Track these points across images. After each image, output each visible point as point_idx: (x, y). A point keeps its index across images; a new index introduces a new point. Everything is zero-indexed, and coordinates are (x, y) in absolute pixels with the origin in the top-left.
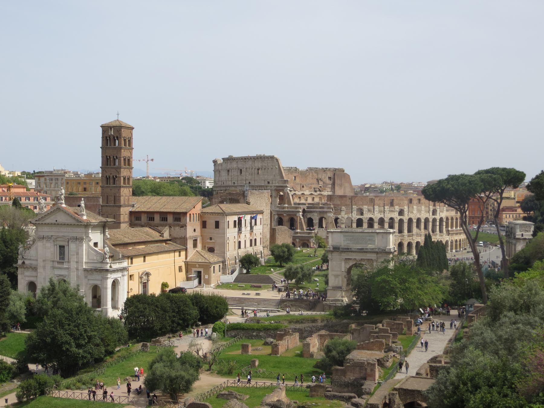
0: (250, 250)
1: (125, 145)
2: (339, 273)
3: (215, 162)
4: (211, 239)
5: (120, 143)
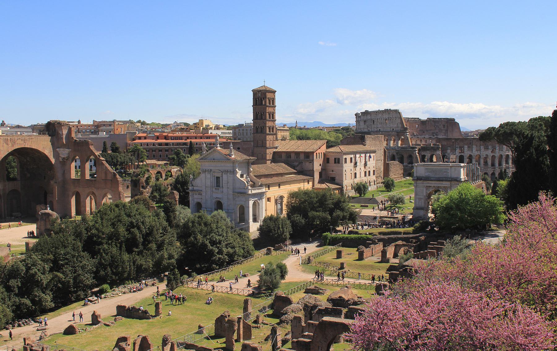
0: (364, 179)
2: (422, 197)
3: (356, 115)
5: (265, 102)
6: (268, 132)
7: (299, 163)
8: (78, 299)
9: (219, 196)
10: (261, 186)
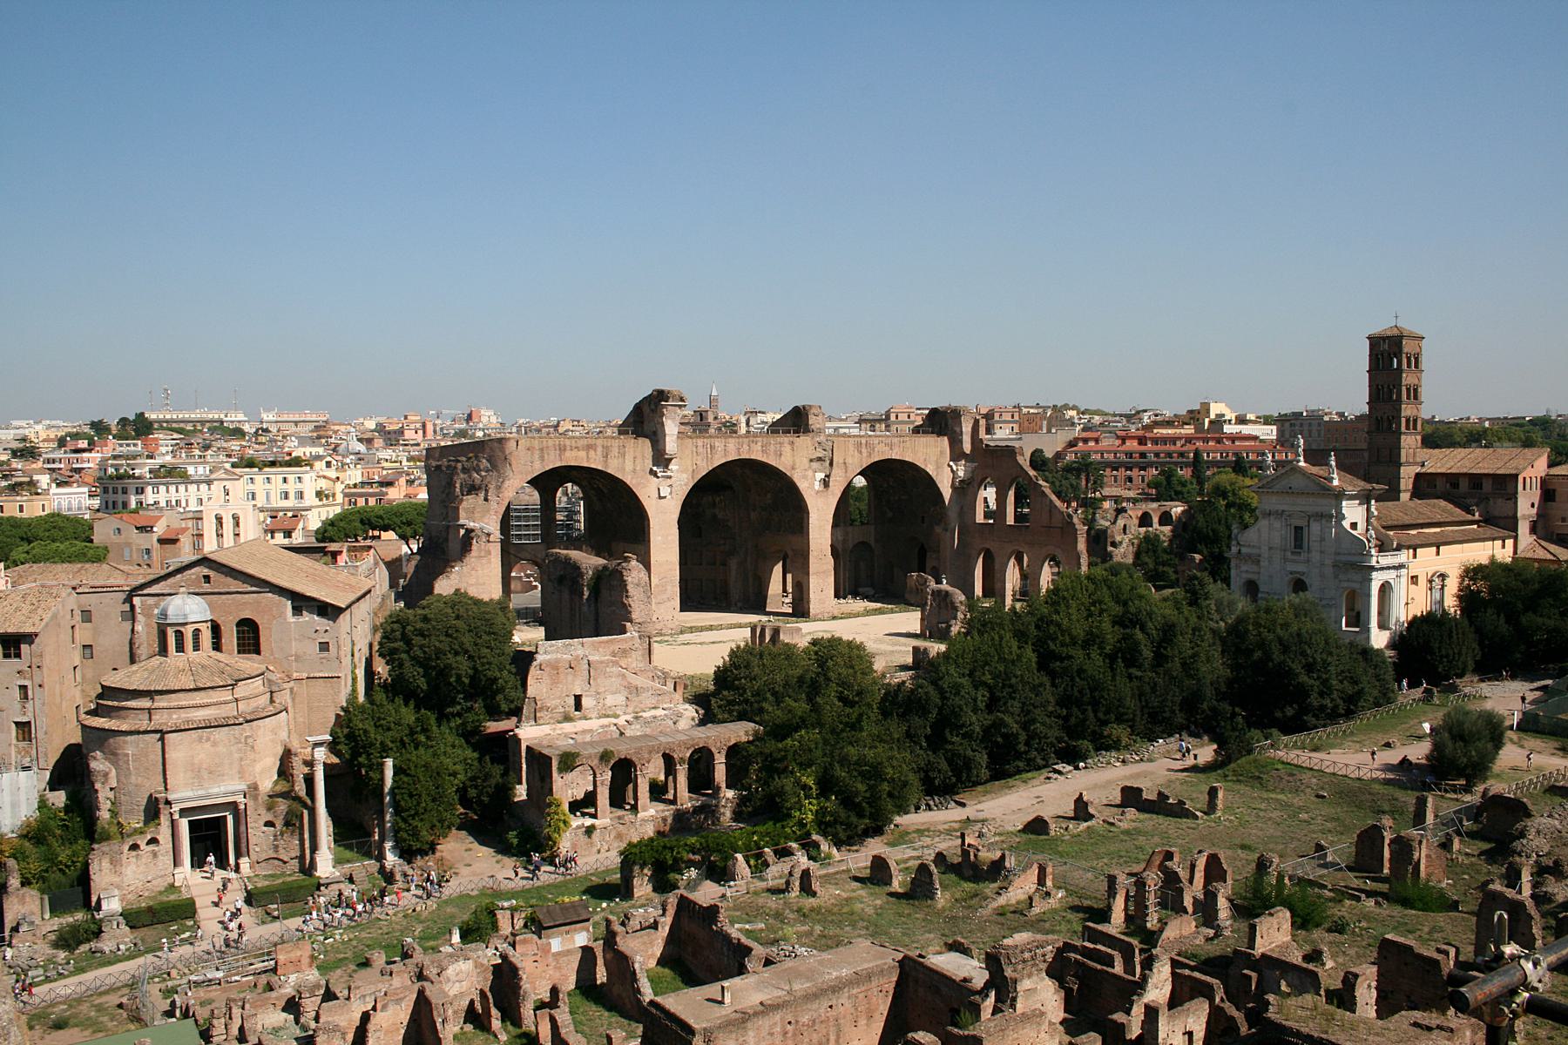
1: (1409, 365)
4: (1564, 520)
5: (1400, 363)
6: (1403, 429)
7: (1484, 500)
8: (1033, 767)
9: (1301, 568)
10: (1399, 548)
